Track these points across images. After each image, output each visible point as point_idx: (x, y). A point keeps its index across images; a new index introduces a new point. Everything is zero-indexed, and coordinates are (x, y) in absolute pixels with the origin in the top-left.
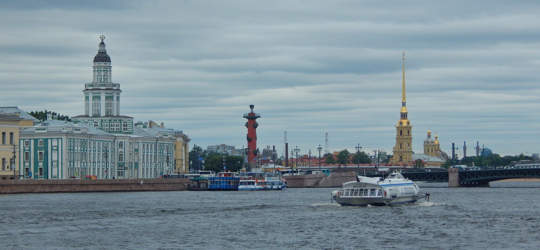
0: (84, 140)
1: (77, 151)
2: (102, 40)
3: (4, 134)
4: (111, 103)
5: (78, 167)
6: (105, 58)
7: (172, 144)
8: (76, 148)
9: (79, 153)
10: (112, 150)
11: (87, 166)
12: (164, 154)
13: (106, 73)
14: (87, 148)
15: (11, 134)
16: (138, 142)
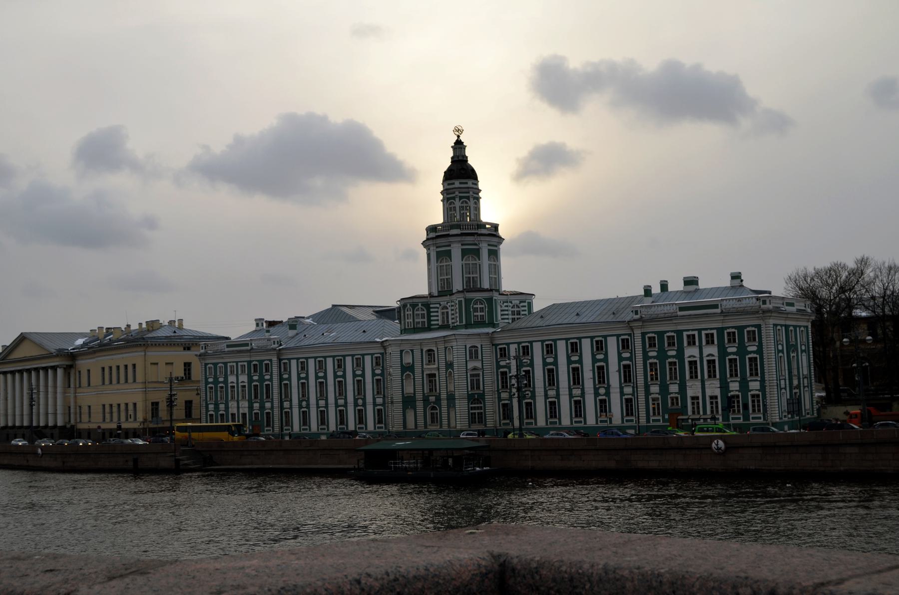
0: (261, 362)
1: (235, 385)
2: (458, 137)
3: (103, 369)
4: (476, 264)
5: (241, 411)
6: (463, 172)
7: (759, 327)
8: (232, 379)
9: (244, 386)
10: (378, 372)
11: (272, 408)
12: (687, 360)
13: (466, 202)
14: (271, 375)
15: (134, 366)
16: (452, 347)
